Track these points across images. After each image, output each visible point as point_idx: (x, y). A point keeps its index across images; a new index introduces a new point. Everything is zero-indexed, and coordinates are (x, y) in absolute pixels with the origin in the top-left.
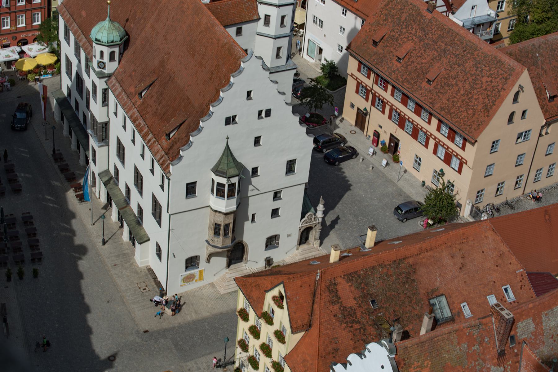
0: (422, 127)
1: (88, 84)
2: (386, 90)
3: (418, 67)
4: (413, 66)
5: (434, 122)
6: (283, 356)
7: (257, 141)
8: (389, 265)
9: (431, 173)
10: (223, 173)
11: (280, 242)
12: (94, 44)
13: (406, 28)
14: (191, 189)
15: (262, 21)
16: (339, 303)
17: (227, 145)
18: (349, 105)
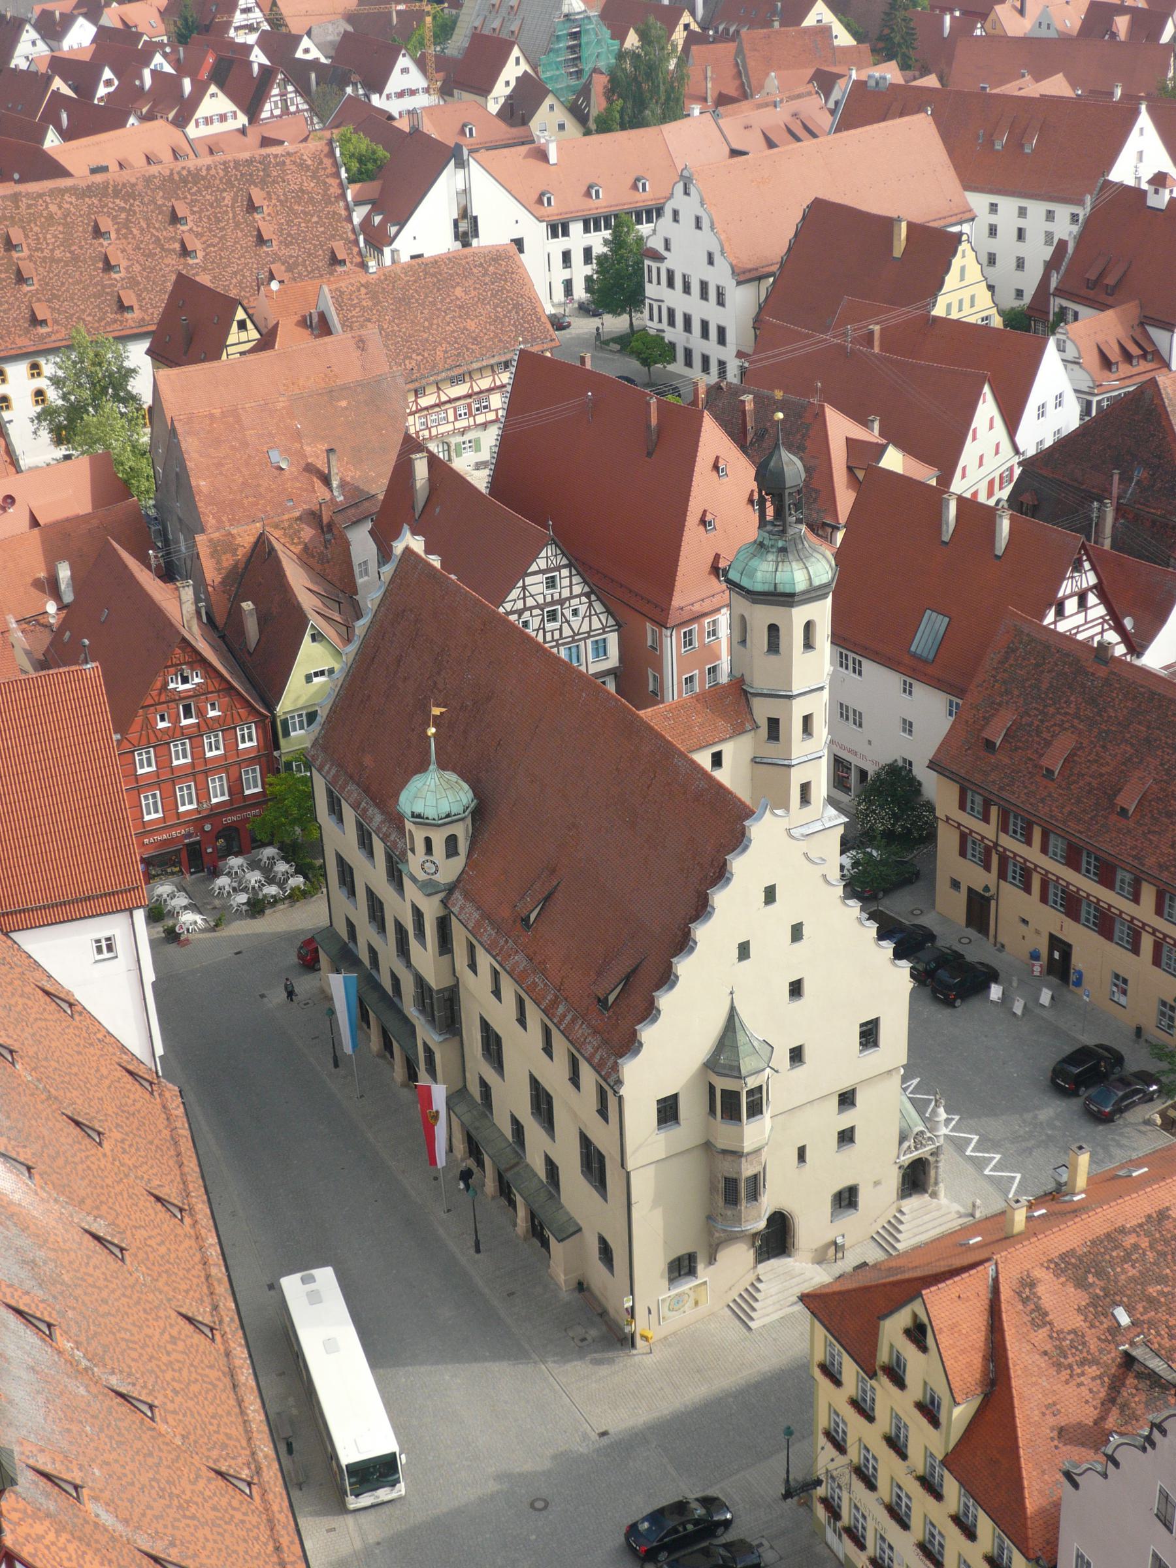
0: (1121, 912)
1: (397, 908)
2: (1029, 842)
3: (1094, 783)
4: (1081, 783)
5: (1148, 894)
6: (940, 1457)
7: (796, 989)
8: (1141, 1225)
9: (1155, 1006)
10: (731, 1068)
11: (863, 1198)
12: (409, 826)
13: (1054, 703)
14: (668, 1111)
15: (764, 730)
16: (1045, 1324)
17: (733, 1009)
18: (948, 883)
